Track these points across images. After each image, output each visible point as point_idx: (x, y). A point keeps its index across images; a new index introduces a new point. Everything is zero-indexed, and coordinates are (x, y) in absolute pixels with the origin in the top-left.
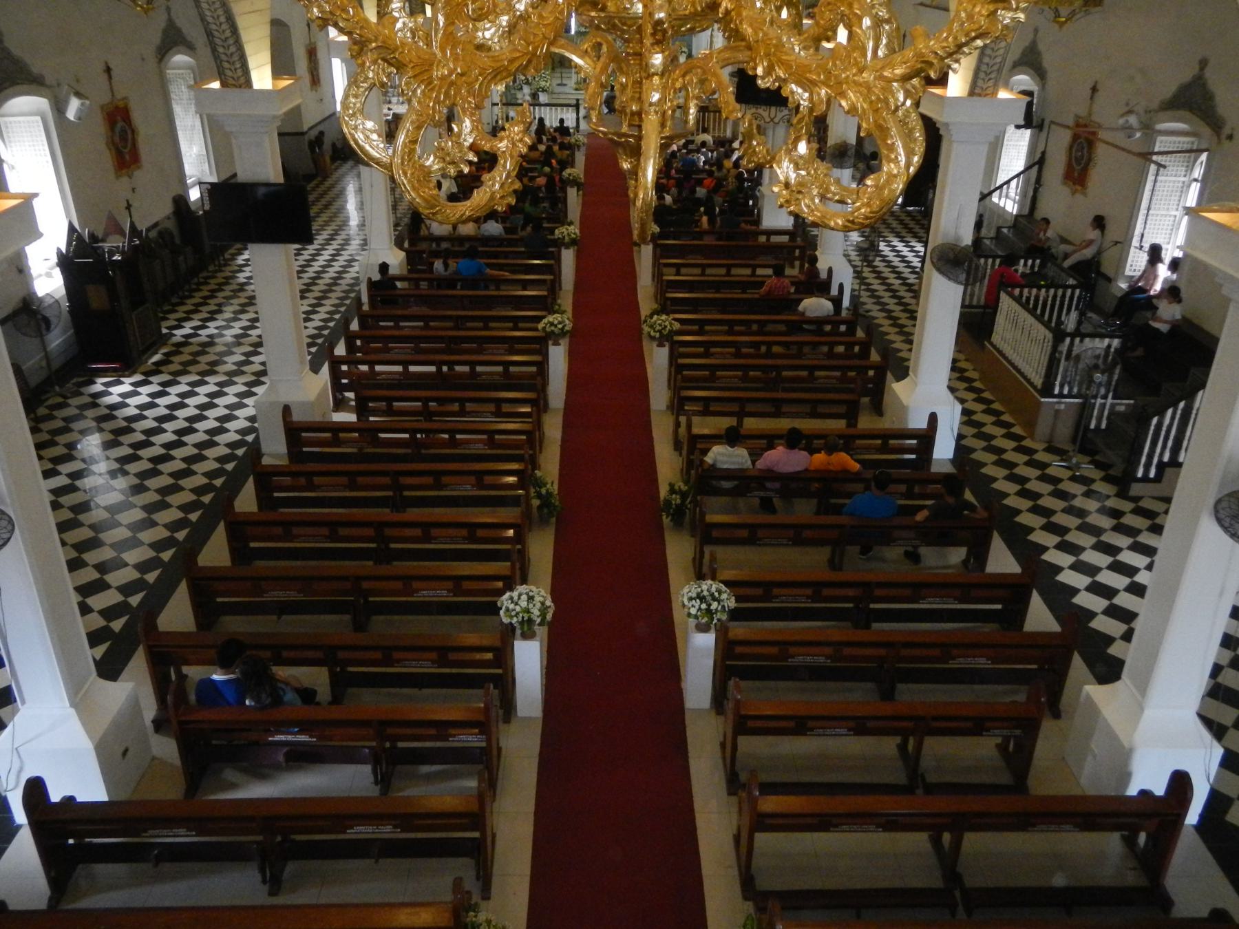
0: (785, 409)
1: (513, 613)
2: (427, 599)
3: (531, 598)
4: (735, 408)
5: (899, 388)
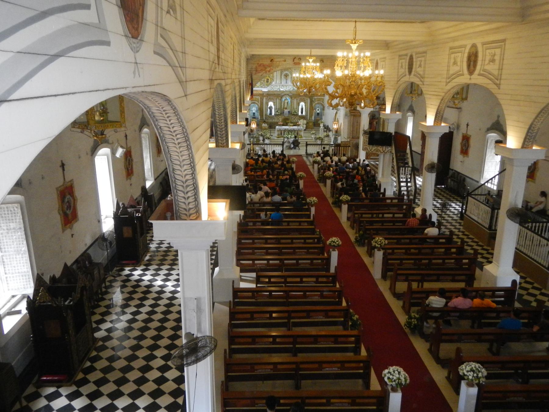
0: (441, 277)
1: (393, 380)
2: (328, 372)
3: (399, 373)
4: (419, 278)
5: (488, 267)
